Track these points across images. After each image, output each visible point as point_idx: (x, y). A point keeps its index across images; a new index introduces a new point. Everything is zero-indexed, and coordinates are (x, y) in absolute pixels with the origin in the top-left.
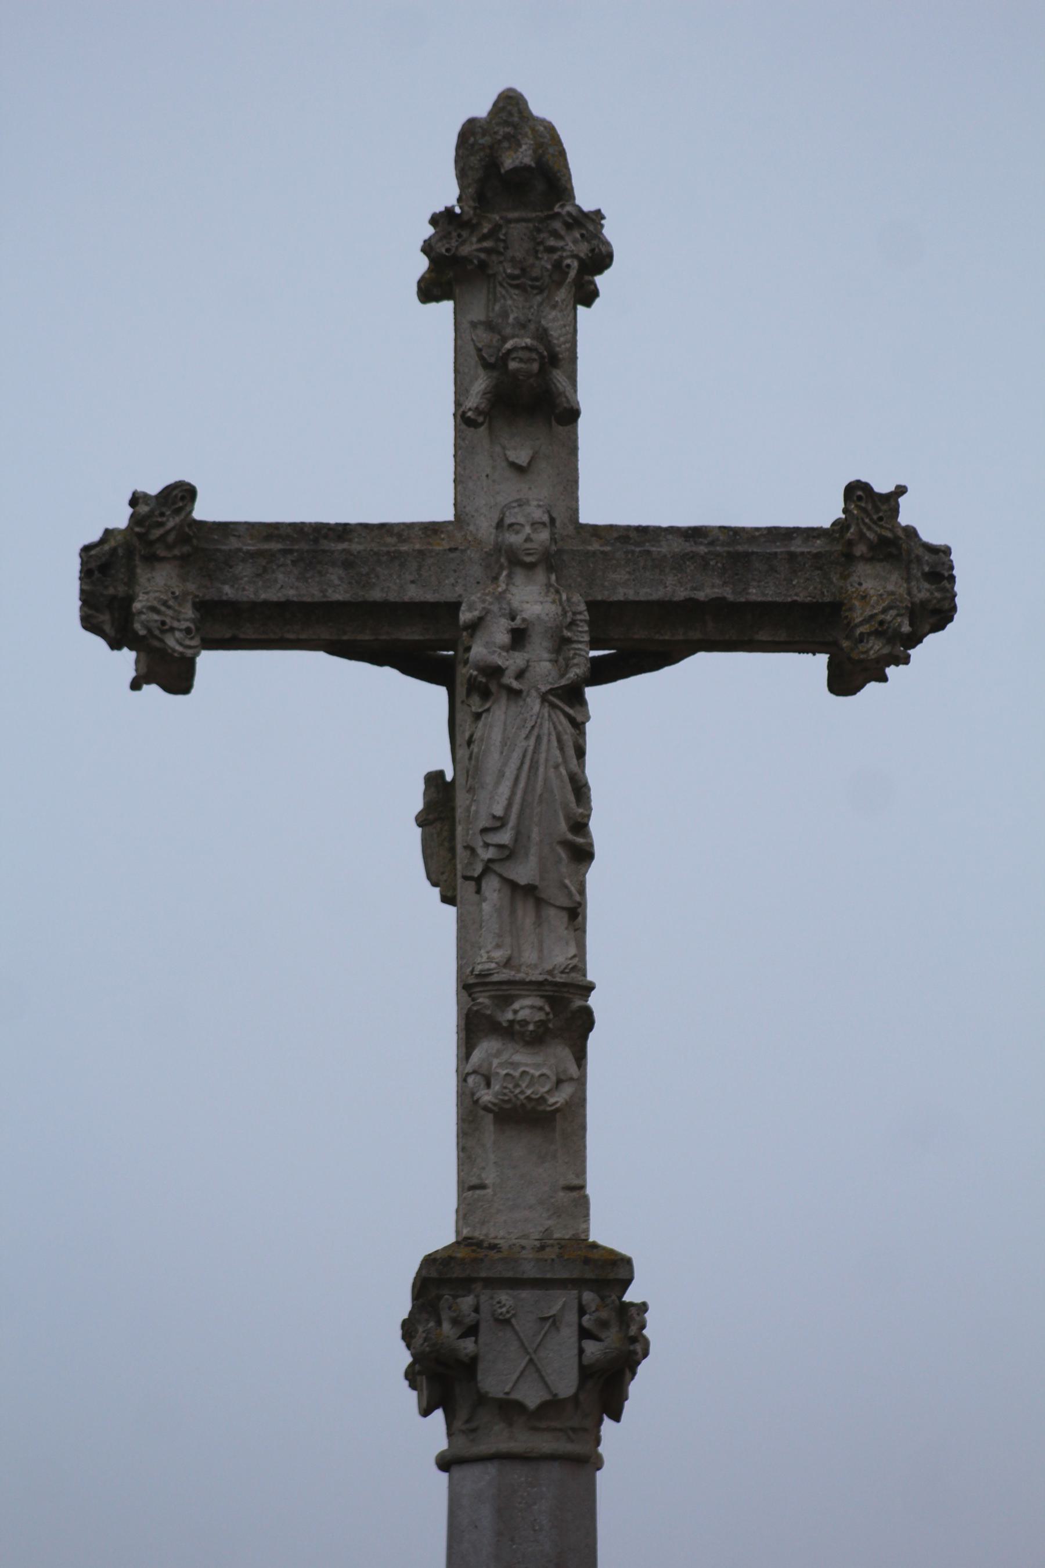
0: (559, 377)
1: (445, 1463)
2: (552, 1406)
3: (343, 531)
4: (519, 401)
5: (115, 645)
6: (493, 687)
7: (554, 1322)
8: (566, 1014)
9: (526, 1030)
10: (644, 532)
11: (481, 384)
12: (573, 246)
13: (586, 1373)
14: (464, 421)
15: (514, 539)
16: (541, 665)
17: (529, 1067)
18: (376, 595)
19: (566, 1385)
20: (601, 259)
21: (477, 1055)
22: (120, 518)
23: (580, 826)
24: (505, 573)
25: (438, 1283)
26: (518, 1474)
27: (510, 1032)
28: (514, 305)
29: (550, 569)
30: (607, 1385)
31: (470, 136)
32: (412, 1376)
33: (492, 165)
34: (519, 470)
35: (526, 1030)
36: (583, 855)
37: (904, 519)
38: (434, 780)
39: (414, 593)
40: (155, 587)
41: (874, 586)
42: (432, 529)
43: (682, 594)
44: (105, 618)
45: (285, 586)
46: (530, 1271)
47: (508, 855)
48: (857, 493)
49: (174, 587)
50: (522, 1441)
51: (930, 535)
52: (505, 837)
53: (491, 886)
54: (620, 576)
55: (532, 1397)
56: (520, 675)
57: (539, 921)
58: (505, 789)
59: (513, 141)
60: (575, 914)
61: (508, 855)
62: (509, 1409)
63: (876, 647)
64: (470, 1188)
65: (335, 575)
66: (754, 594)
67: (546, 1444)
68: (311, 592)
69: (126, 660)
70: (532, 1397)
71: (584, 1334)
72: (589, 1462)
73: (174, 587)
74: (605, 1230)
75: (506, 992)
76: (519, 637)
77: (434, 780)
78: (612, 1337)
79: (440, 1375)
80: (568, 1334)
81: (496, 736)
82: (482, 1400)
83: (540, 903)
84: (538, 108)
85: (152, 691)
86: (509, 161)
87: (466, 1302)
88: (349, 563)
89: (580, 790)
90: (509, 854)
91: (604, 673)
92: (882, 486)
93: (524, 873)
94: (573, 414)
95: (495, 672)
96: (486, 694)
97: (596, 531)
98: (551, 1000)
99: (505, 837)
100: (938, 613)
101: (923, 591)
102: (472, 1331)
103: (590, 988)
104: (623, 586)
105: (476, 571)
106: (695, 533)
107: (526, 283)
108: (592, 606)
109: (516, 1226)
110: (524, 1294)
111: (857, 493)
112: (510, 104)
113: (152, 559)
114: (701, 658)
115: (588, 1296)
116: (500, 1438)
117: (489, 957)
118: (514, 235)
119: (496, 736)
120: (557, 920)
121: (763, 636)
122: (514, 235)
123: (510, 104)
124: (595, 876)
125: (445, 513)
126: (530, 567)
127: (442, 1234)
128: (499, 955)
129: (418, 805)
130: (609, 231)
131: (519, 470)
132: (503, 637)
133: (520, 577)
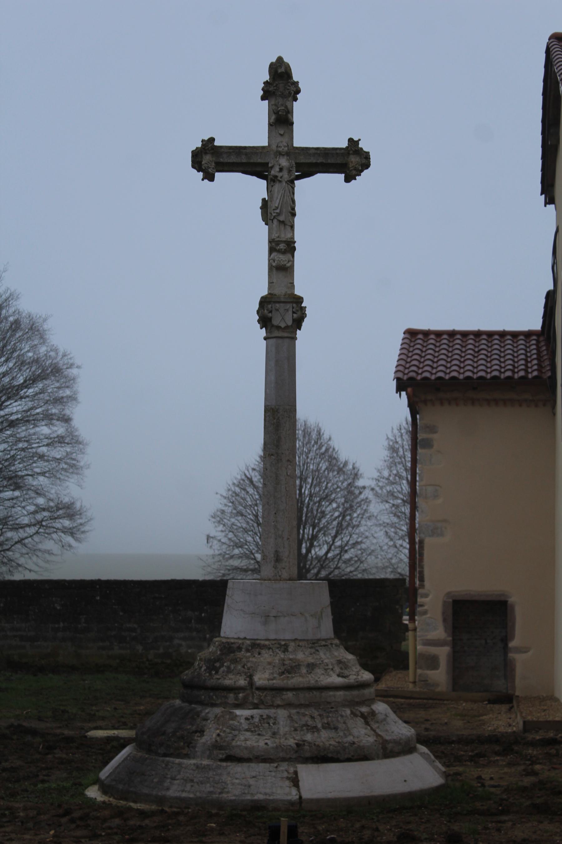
0: (289, 116)
1: (265, 339)
2: (287, 327)
3: (245, 148)
4: (281, 121)
5: (198, 171)
7: (287, 310)
8: (290, 248)
9: (282, 251)
11: (273, 117)
12: (293, 88)
13: (294, 320)
14: (270, 125)
15: (280, 149)
16: (285, 175)
17: (282, 258)
18: (252, 161)
19: (290, 323)
20: (298, 91)
22: (199, 145)
23: (293, 209)
25: (264, 302)
26: (280, 341)
27: (279, 251)
28: (280, 100)
30: (298, 323)
31: (272, 66)
32: (259, 321)
33: (276, 72)
34: (281, 135)
35: (282, 251)
36: (294, 215)
37: (360, 146)
38: (264, 200)
40: (207, 159)
41: (354, 160)
42: (263, 148)
43: (314, 161)
44: (196, 166)
45: (233, 159)
46: (282, 300)
47: (279, 216)
48: (351, 140)
49: (211, 159)
50: (281, 334)
51: (365, 149)
52: (278, 211)
55: (283, 325)
56: (281, 177)
57: (285, 228)
58: (278, 201)
59: (280, 67)
60: (292, 227)
61: (279, 216)
62: (278, 328)
63: (354, 172)
64: (270, 283)
65: (243, 157)
66: (329, 161)
67: (285, 335)
68: (238, 160)
69: (201, 174)
71: (293, 312)
72: (295, 338)
73: (211, 159)
74: (298, 292)
75: (278, 243)
76: (281, 170)
77: (264, 200)
78: (299, 313)
79: (265, 321)
80: (290, 313)
81: (276, 190)
82: (273, 326)
84: (286, 60)
85: (206, 181)
86: (279, 71)
87: (270, 306)
88: (246, 154)
89: (293, 202)
90: (279, 214)
91: (298, 178)
92: (356, 139)
93: (282, 218)
94: (292, 124)
96: (274, 181)
97: (297, 148)
99: (278, 211)
100: (367, 165)
101: (364, 161)
102: (271, 312)
103: (295, 242)
104: (302, 160)
106: (317, 149)
107: (283, 96)
108: (296, 163)
109: (280, 291)
110: (282, 305)
111: (351, 140)
112: (280, 59)
113: (206, 153)
115: (294, 305)
116: (276, 333)
118: (280, 86)
119: (276, 190)
120: (289, 228)
121: (331, 170)
122: (280, 86)
123: (280, 59)
124: (296, 219)
125: (267, 144)
126: (283, 155)
127: (265, 292)
128: (277, 235)
129: (261, 205)
130: (300, 86)
131: (281, 135)
132: (278, 169)
133: (281, 157)
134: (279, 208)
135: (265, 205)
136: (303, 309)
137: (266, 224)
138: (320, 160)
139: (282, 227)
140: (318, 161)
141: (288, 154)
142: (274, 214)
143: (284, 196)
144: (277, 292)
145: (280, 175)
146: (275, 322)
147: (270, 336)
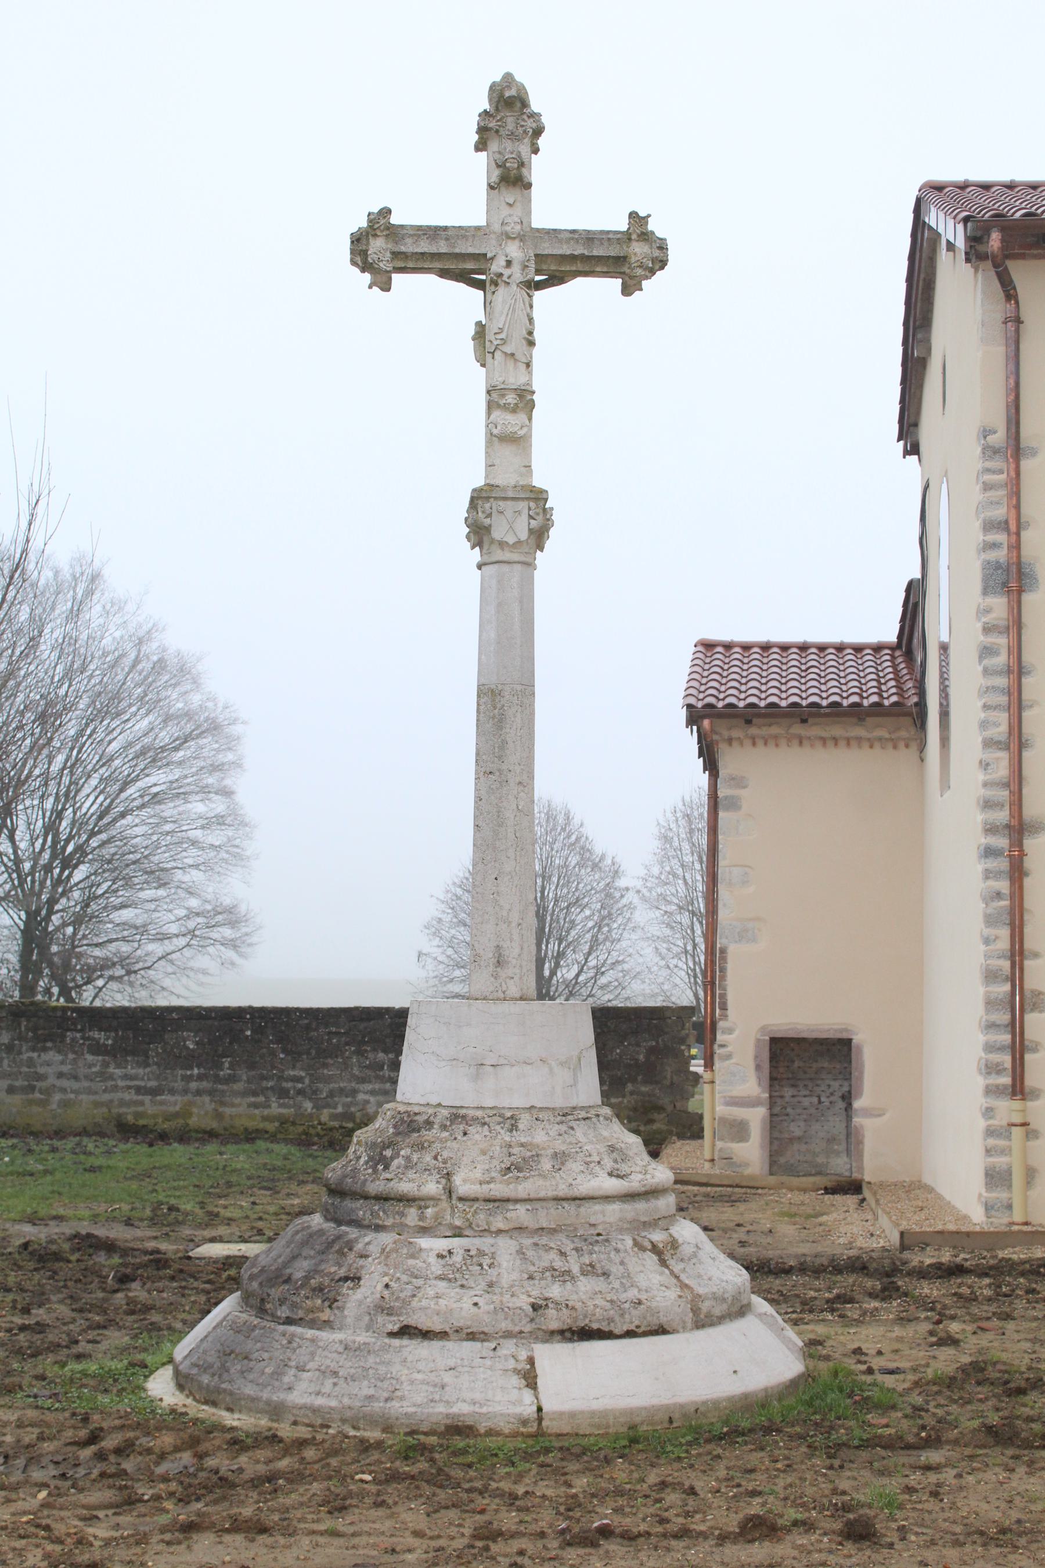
6: (499, 281)
10: (555, 230)
15: (508, 228)
17: (511, 422)
18: (457, 251)
21: (492, 417)
23: (531, 333)
24: (753, 1447)
29: (521, 240)
34: (510, 205)
36: (531, 344)
38: (479, 324)
39: (471, 250)
43: (568, 252)
52: (503, 336)
53: (498, 354)
54: (546, 245)
56: (509, 277)
57: (515, 368)
58: (503, 318)
60: (528, 365)
65: (442, 243)
75: (503, 392)
76: (509, 263)
77: (479, 324)
81: (500, 299)
83: (516, 360)
88: (447, 239)
89: (531, 320)
90: (504, 341)
91: (539, 286)
93: (508, 349)
95: (501, 275)
96: (496, 285)
97: (538, 230)
98: (521, 397)
103: (534, 392)
104: (547, 248)
105: (494, 242)
106: (574, 232)
108: (536, 255)
114: (580, 281)
117: (498, 380)
119: (500, 299)
120: (523, 367)
124: (536, 351)
125: (483, 223)
126: (514, 238)
128: (501, 379)
129: (473, 333)
131: (510, 205)
132: (504, 263)
133: (510, 242)
134: (505, 330)
135: (480, 332)
137: (483, 365)
138: (579, 250)
139: (511, 364)
140: (576, 253)
141: (521, 238)
142: (498, 342)
143: (514, 310)
145: (506, 272)
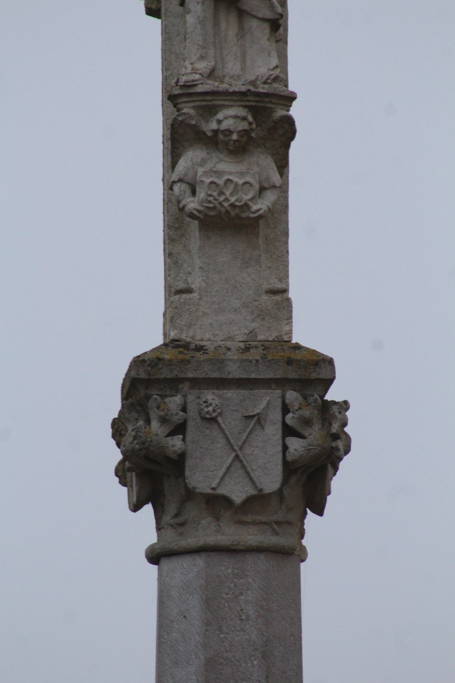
1: (155, 556)
2: (258, 500)
7: (259, 420)
8: (268, 124)
13: (290, 468)
19: (271, 481)
25: (146, 383)
26: (225, 566)
27: (214, 141)
30: (310, 481)
32: (121, 473)
46: (234, 371)
55: (238, 492)
57: (241, 34)
62: (216, 503)
64: (177, 292)
67: (251, 537)
70: (238, 492)
71: (288, 431)
72: (294, 554)
74: (306, 332)
75: (210, 103)
78: (315, 434)
79: (150, 473)
80: (273, 431)
82: (190, 495)
102: (180, 429)
103: (292, 98)
109: (223, 328)
110: (231, 394)
115: (292, 396)
116: (208, 532)
117: (194, 68)
120: (260, 32)
127: (149, 336)
128: (202, 66)
136: (332, 416)
144: (206, 332)
146: (203, 476)
147: (175, 541)
